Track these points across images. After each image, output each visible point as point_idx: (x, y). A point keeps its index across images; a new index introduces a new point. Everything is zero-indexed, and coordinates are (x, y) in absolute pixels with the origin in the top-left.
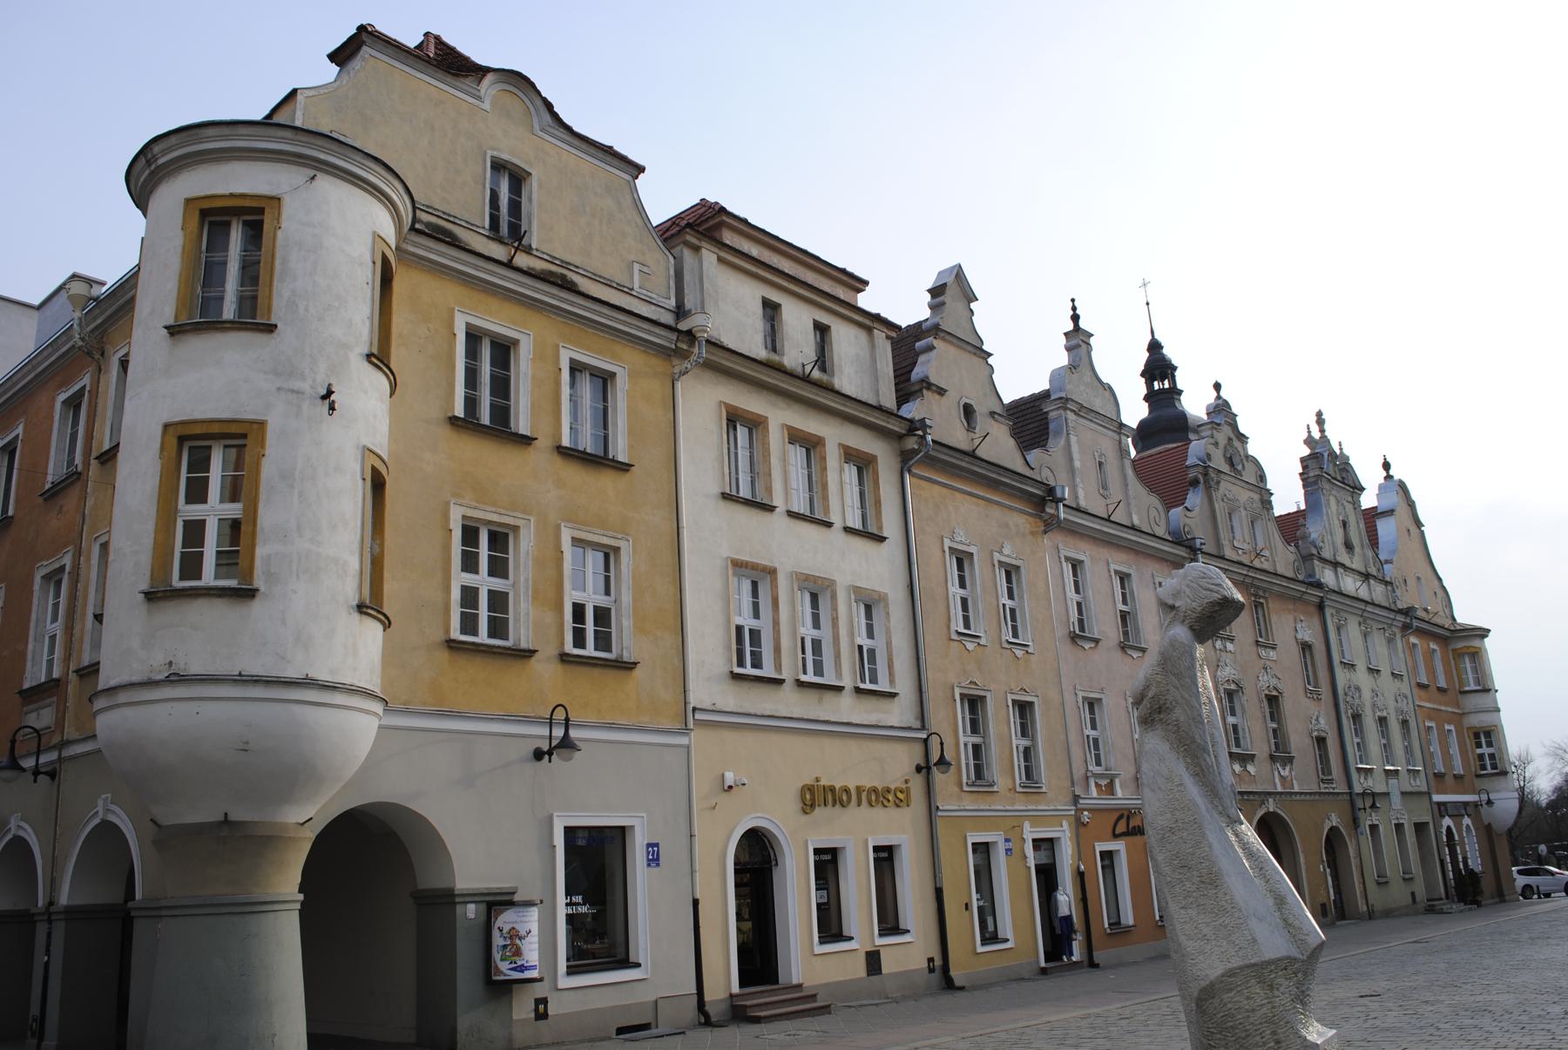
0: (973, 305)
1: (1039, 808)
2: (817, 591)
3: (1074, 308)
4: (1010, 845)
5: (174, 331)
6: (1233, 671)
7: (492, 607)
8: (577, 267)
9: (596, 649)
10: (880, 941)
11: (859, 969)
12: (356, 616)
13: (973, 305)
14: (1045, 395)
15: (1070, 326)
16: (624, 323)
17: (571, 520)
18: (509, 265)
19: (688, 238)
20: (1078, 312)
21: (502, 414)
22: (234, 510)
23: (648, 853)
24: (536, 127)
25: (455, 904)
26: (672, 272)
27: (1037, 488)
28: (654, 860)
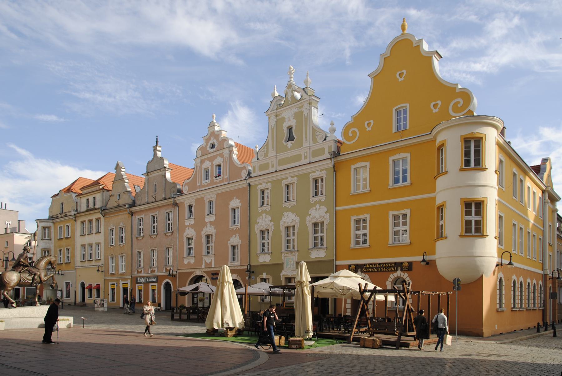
2: (91, 245)
4: (117, 284)
7: (403, 173)
10: (96, 299)
11: (93, 302)
20: (158, 140)
28: (71, 286)
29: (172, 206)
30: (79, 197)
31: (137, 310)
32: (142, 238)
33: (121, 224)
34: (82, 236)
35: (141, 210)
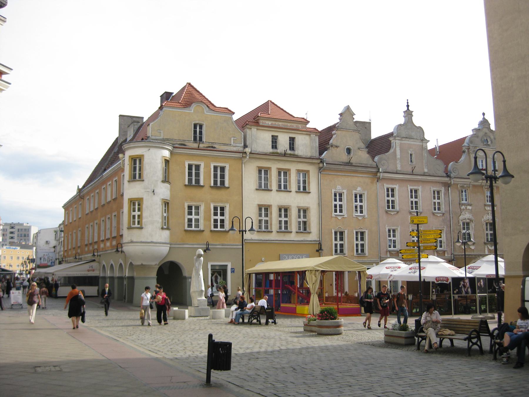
0: (354, 117)
1: (363, 260)
3: (408, 103)
5: (129, 181)
6: (469, 216)
8: (216, 143)
9: (220, 228)
12: (161, 230)
13: (354, 117)
14: (391, 134)
15: (406, 109)
16: (228, 154)
17: (213, 201)
18: (198, 149)
19: (247, 127)
21: (198, 181)
22: (139, 213)
23: (231, 270)
24: (205, 112)
25: (186, 279)
26: (243, 137)
27: (374, 169)
29: (441, 185)
30: (256, 128)
31: (155, 319)
32: (395, 213)
33: (359, 189)
34: (258, 191)
35: (393, 178)
